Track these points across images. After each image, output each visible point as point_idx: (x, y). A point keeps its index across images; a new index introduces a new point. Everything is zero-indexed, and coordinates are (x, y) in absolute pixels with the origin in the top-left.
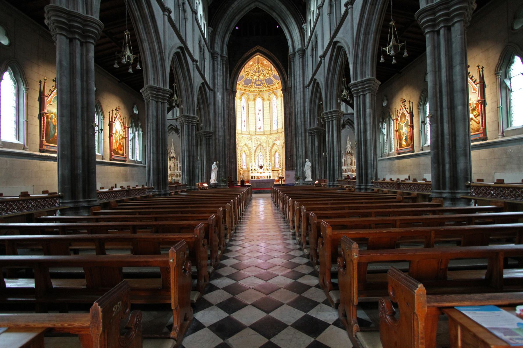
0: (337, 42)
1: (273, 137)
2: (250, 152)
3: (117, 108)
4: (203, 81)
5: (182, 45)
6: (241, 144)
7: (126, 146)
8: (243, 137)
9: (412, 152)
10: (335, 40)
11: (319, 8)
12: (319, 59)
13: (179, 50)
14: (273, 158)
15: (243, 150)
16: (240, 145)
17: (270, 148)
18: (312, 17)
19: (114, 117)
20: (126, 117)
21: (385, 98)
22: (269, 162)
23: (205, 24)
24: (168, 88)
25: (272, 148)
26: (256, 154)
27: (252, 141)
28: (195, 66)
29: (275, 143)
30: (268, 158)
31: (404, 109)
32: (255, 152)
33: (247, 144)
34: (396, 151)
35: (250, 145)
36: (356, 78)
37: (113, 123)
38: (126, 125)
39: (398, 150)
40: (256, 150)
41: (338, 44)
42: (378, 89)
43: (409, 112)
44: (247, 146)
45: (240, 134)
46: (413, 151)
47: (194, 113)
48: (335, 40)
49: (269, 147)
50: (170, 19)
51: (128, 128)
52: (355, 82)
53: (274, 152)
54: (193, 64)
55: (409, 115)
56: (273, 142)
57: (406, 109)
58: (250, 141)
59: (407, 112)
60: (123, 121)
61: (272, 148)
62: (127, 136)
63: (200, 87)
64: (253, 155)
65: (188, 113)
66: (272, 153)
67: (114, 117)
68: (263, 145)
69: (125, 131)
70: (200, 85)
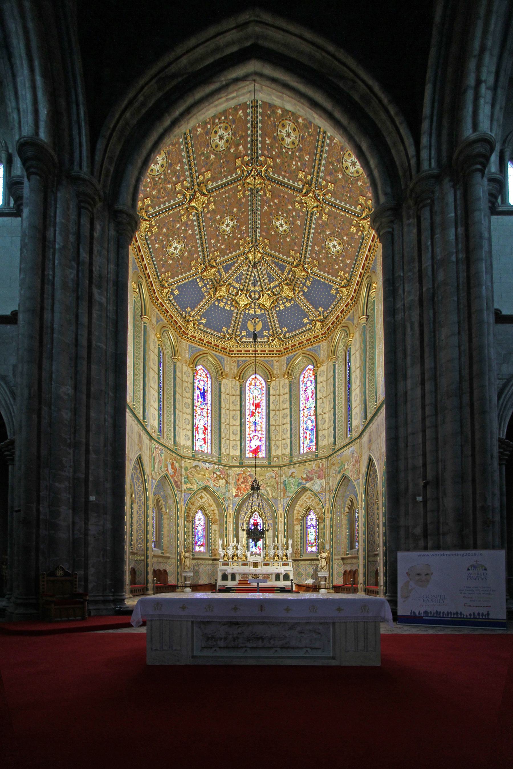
1: (300, 472)
2: (223, 511)
6: (189, 486)
8: (197, 466)
14: (297, 528)
15: (197, 504)
16: (184, 487)
17: (287, 501)
22: (285, 537)
25: (294, 500)
26: (240, 518)
27: (227, 482)
29: (307, 485)
30: (281, 527)
32: (238, 512)
33: (212, 488)
35: (220, 493)
40: (240, 506)
44: (212, 494)
45: (187, 458)
49: (284, 497)
53: (303, 510)
56: (299, 483)
58: (222, 482)
61: (294, 500)
64: (231, 519)
66: (295, 515)
68: (265, 493)
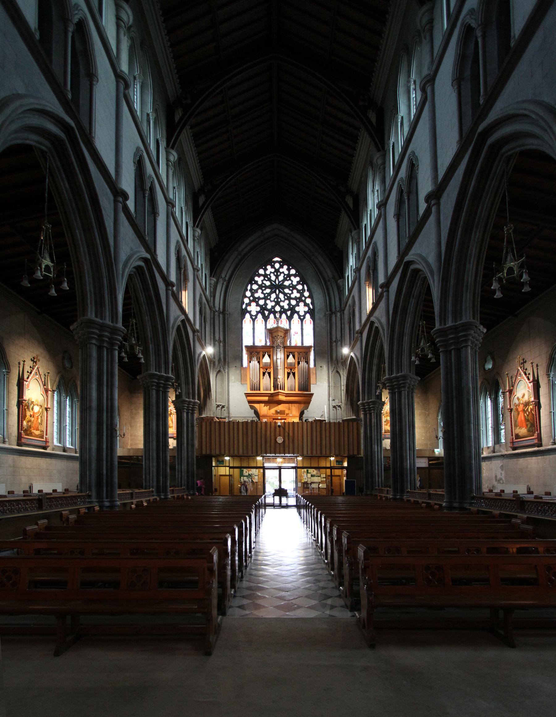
0: (409, 263)
3: (34, 358)
4: (183, 317)
5: (148, 256)
7: (49, 422)
9: (538, 447)
10: (407, 259)
11: (379, 207)
12: (380, 290)
13: (142, 264)
18: (367, 222)
19: (28, 372)
20: (48, 373)
21: (489, 357)
24: (120, 325)
28: (170, 292)
31: (524, 375)
34: (510, 445)
36: (443, 320)
37: (25, 382)
38: (49, 387)
39: (513, 442)
41: (412, 267)
42: (481, 341)
43: (531, 379)
46: (541, 445)
47: (167, 371)
48: (407, 259)
50: (126, 209)
51: (53, 391)
52: (442, 327)
54: (167, 290)
55: (532, 384)
57: (525, 374)
59: (529, 379)
60: (43, 380)
62: (49, 406)
63: (179, 326)
65: (157, 369)
67: (28, 372)
69: (47, 396)
70: (179, 323)
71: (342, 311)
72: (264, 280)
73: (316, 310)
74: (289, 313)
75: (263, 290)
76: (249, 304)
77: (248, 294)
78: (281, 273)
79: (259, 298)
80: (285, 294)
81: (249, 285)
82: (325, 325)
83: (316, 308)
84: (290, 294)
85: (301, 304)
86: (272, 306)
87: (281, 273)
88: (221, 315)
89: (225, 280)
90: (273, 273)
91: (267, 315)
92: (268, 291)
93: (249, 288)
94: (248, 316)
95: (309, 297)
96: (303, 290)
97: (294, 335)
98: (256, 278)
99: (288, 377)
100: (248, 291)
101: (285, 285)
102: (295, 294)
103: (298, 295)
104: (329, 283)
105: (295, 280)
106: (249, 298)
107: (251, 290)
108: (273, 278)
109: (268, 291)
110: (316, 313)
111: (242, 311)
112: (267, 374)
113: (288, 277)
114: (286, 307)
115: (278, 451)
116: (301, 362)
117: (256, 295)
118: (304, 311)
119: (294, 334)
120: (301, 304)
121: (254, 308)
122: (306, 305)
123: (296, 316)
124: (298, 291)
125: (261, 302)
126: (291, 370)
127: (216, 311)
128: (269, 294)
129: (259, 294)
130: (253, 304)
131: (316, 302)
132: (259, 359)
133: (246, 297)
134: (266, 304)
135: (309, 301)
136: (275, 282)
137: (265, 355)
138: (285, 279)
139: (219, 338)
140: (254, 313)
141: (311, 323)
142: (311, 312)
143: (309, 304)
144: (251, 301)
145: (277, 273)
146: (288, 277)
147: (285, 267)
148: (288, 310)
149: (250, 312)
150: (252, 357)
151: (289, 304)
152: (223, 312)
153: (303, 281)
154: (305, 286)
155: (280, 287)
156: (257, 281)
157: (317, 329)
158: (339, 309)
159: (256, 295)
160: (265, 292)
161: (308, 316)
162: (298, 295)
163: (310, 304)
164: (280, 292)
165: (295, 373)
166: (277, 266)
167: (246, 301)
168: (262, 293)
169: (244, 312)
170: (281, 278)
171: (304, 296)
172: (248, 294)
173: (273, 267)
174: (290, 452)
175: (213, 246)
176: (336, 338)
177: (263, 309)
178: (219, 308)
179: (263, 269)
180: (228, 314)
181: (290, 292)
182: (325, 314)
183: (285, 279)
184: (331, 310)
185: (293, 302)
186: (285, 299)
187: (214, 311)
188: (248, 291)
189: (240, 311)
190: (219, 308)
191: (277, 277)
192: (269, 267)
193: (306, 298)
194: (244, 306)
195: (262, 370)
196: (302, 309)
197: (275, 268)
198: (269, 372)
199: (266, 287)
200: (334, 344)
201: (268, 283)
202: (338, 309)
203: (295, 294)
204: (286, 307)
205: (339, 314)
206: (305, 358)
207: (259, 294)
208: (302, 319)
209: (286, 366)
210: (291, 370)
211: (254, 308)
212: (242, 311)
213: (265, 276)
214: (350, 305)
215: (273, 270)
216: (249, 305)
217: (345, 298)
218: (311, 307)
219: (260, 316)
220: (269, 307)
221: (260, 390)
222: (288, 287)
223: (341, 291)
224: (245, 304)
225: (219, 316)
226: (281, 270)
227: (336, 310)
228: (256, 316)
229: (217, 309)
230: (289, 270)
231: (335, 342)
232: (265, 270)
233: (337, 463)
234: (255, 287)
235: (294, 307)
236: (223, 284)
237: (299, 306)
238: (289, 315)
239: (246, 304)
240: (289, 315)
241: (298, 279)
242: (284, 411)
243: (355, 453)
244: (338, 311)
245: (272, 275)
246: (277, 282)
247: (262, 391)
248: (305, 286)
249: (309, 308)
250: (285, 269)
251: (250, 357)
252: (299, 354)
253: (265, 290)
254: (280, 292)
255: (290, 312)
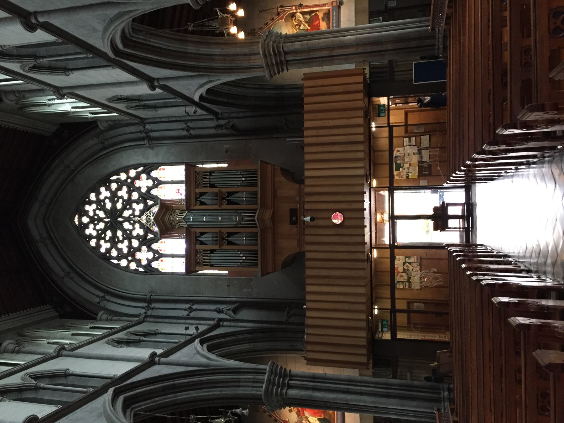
23: (92, 326)
71: (143, 121)
72: (104, 239)
73: (145, 161)
74: (150, 203)
75: (119, 241)
76: (138, 262)
77: (124, 263)
78: (95, 214)
79: (130, 247)
80: (124, 208)
81: (112, 261)
82: (165, 148)
83: (139, 162)
84: (124, 200)
85: (138, 183)
86: (140, 228)
87: (95, 214)
88: (153, 305)
89: (104, 297)
90: (95, 225)
91: (152, 236)
92: (119, 233)
93: (115, 262)
94: (154, 264)
95: (127, 172)
96: (117, 181)
97: (181, 195)
98: (103, 250)
99: (235, 203)
100: (119, 262)
101: (111, 208)
102: (123, 193)
103: (125, 189)
104: (106, 143)
105: (104, 193)
106: (129, 262)
107: (119, 258)
108: (101, 226)
109: (119, 233)
110: (149, 161)
111: (147, 272)
112: (231, 239)
113: (100, 204)
114: (141, 206)
115: (358, 222)
116: (211, 183)
117: (125, 251)
118: (147, 179)
119: (179, 194)
120: (138, 183)
121: (144, 255)
122: (138, 177)
123: (154, 192)
124: (119, 189)
125: (135, 243)
126: (223, 199)
127: (146, 313)
128: (124, 231)
129: (124, 246)
130: (138, 255)
131: (132, 162)
132: (207, 251)
133: (128, 266)
134: (138, 237)
135: (132, 173)
136: (106, 223)
137: (201, 241)
138: (103, 208)
139: (185, 309)
140: (150, 255)
141: (164, 169)
142: (148, 169)
143: (137, 172)
144: (135, 260)
145: (95, 220)
146: (100, 204)
147: (87, 207)
148: (146, 204)
149: (149, 261)
150: (204, 262)
151: (138, 202)
152: (150, 301)
153: (106, 182)
154: (112, 178)
155: (114, 214)
156: (107, 249)
157: (172, 159)
158: (140, 126)
159: (125, 251)
160: (121, 238)
161: (154, 174)
162: (125, 189)
163: (137, 170)
164: (121, 216)
165: (227, 192)
166: (85, 220)
167: (133, 266)
168: (122, 242)
169: (149, 269)
170: (101, 214)
171: (126, 180)
172: (124, 263)
173: (86, 226)
174: (359, 199)
175: (57, 314)
176: (182, 129)
177: (145, 242)
178: (142, 308)
179: (90, 240)
180: (151, 295)
181: (121, 201)
182: (149, 147)
183: (103, 208)
184: (143, 139)
185: (135, 196)
186: (131, 208)
187: (146, 316)
188: (119, 262)
189: (147, 276)
190: (142, 308)
191: (100, 220)
192: (87, 232)
193: (128, 177)
194: (141, 270)
195: (225, 247)
196: (144, 183)
197: (88, 224)
198: (227, 235)
199: (114, 236)
200: (192, 132)
201: (109, 234)
202: (141, 128)
203: (123, 193)
204: (141, 206)
205: (148, 127)
206: (204, 175)
207: (124, 246)
208: (157, 183)
209: (216, 207)
210: (224, 198)
211: (144, 255)
212: (147, 272)
213: (99, 237)
214: (127, 107)
215: (91, 226)
216: (138, 262)
217: (125, 118)
218: (140, 169)
219: (155, 246)
220: (141, 232)
221: (257, 251)
222: (114, 203)
223: (114, 125)
224: (138, 268)
225: (153, 308)
226: (91, 214)
227: (144, 131)
228: (155, 252)
229: (144, 311)
230: (90, 203)
231: (188, 131)
232: (91, 237)
233: (381, 115)
234: (114, 253)
235: (141, 194)
236: (108, 301)
237: (139, 188)
238: (153, 202)
239: (137, 266)
240: (153, 202)
241: (103, 189)
242: (291, 210)
243: (360, 79)
244: (144, 127)
245: (98, 227)
246: (107, 220)
247: (259, 247)
248: (112, 178)
249: (143, 172)
250: (90, 209)
251: (204, 265)
252: (197, 186)
253: (118, 238)
254: (121, 216)
255: (148, 201)
